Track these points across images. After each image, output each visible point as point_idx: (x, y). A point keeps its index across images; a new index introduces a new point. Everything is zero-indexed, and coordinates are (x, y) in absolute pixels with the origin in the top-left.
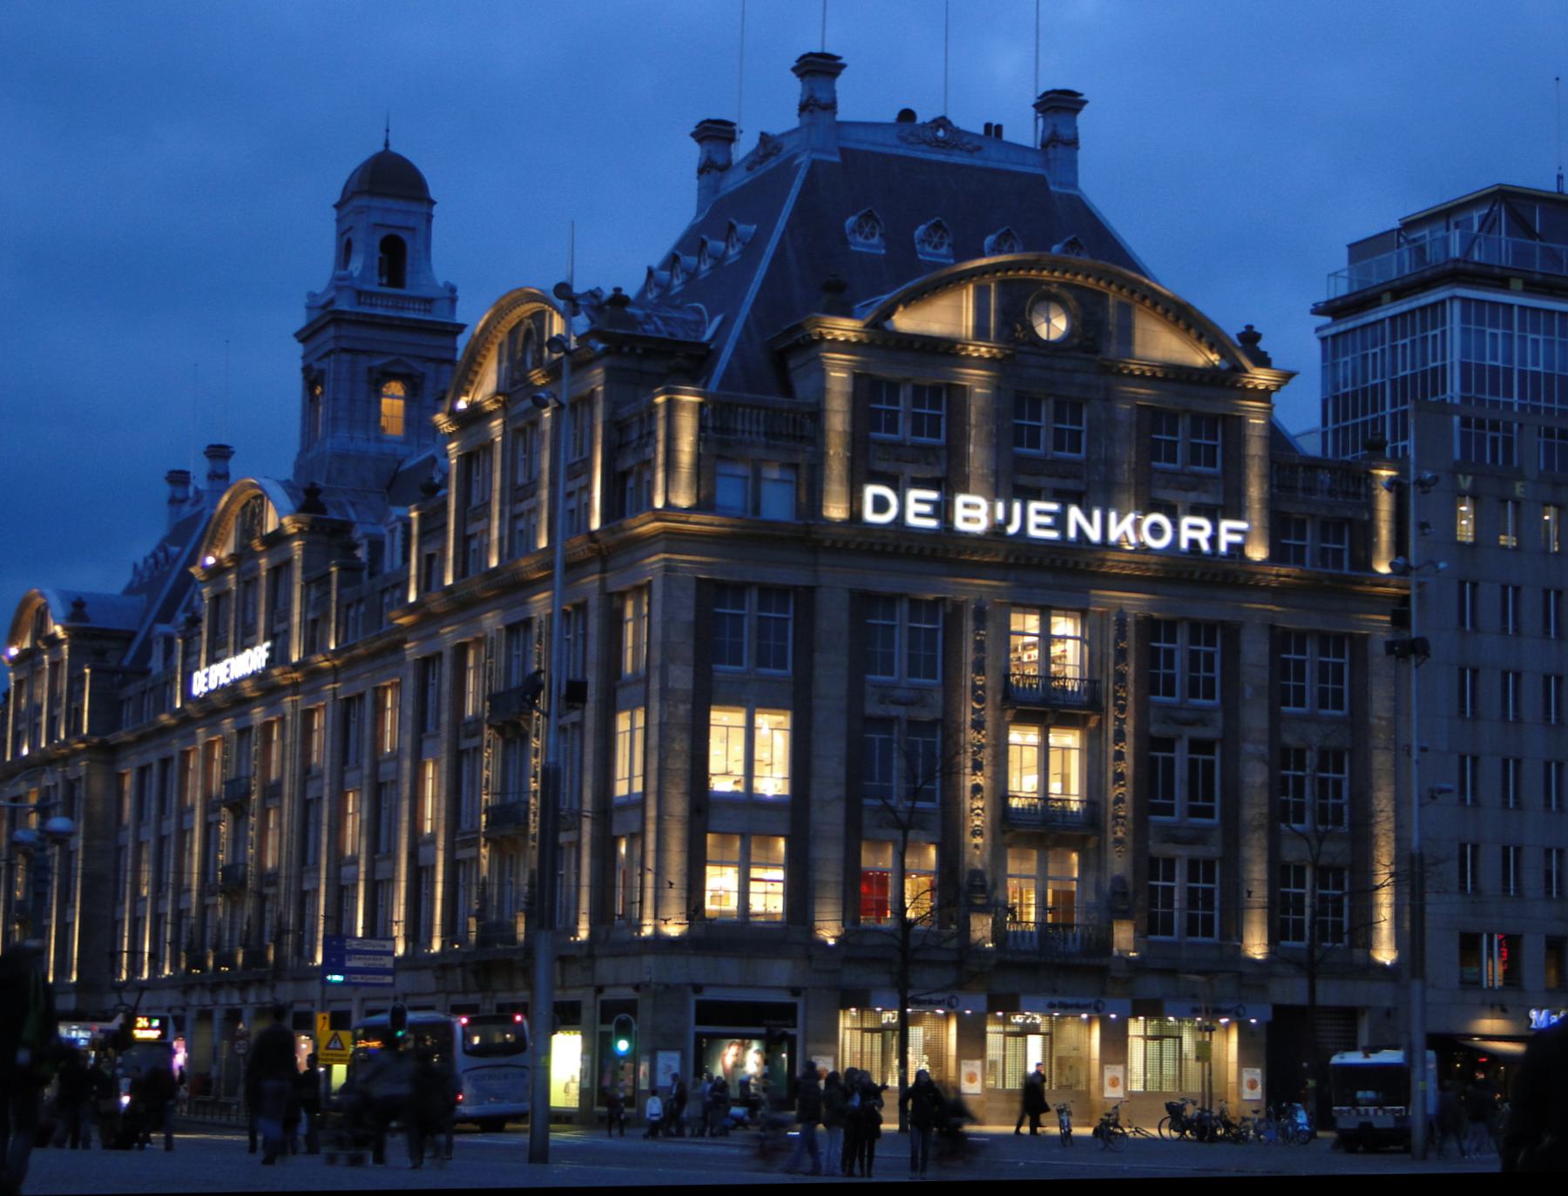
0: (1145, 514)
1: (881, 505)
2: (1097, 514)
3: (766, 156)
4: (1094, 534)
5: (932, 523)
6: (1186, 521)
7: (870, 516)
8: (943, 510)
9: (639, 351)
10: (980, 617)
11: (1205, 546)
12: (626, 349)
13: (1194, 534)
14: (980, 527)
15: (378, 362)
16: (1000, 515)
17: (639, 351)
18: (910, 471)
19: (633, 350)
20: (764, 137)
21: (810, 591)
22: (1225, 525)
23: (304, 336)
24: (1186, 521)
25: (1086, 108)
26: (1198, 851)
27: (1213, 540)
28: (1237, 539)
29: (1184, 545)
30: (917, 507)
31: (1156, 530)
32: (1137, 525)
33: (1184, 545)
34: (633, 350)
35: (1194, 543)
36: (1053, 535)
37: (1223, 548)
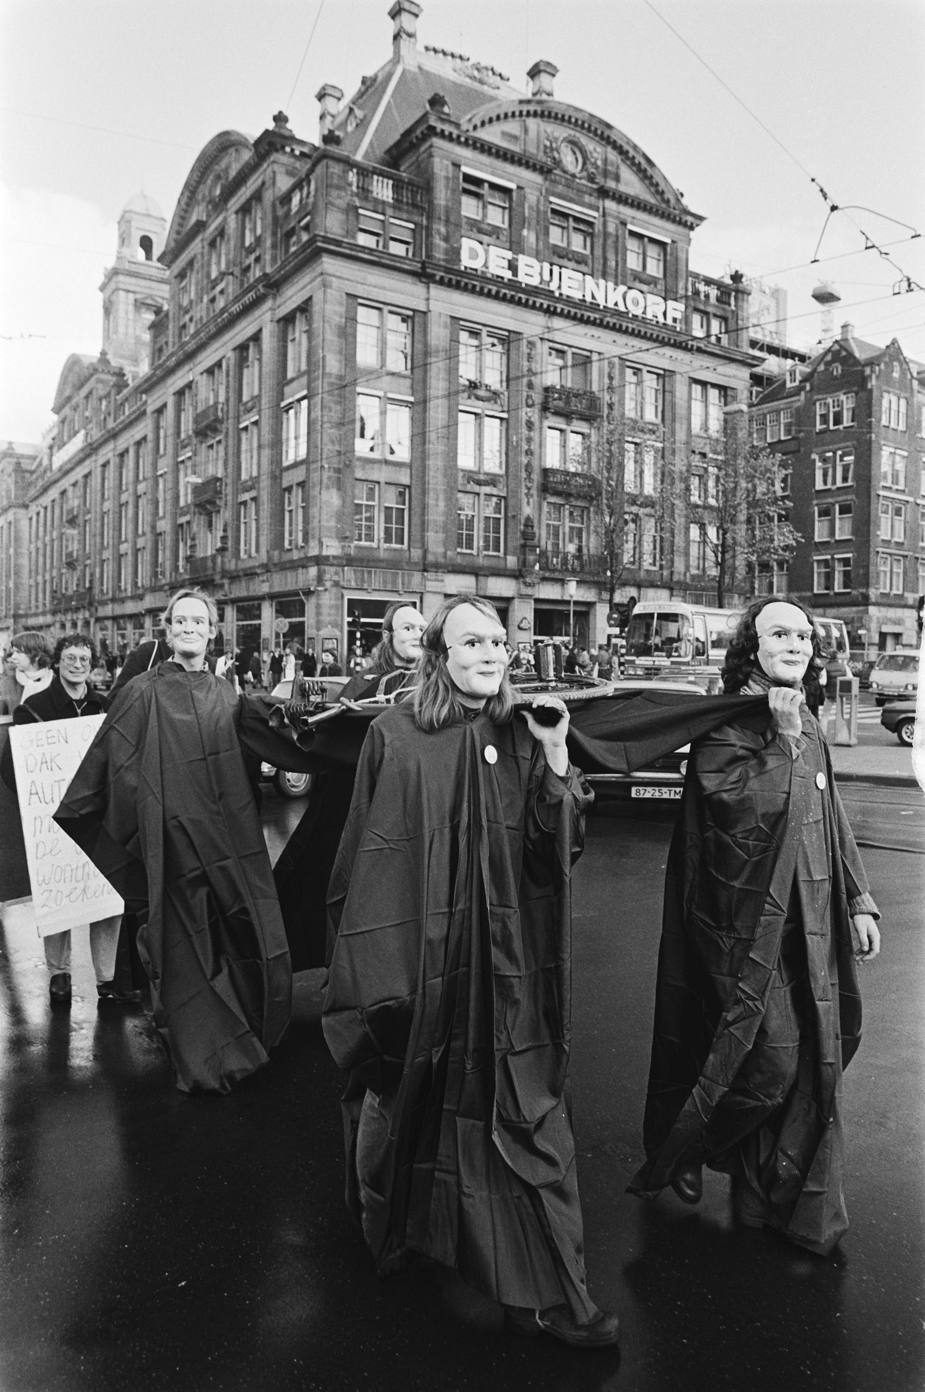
1: (474, 255)
3: (367, 90)
4: (601, 301)
5: (508, 275)
8: (513, 266)
9: (297, 153)
10: (531, 344)
12: (288, 149)
14: (535, 281)
15: (138, 296)
16: (546, 277)
17: (297, 153)
18: (486, 239)
19: (292, 150)
20: (364, 81)
21: (425, 313)
22: (671, 303)
23: (102, 288)
25: (558, 75)
27: (665, 314)
28: (679, 316)
34: (292, 150)
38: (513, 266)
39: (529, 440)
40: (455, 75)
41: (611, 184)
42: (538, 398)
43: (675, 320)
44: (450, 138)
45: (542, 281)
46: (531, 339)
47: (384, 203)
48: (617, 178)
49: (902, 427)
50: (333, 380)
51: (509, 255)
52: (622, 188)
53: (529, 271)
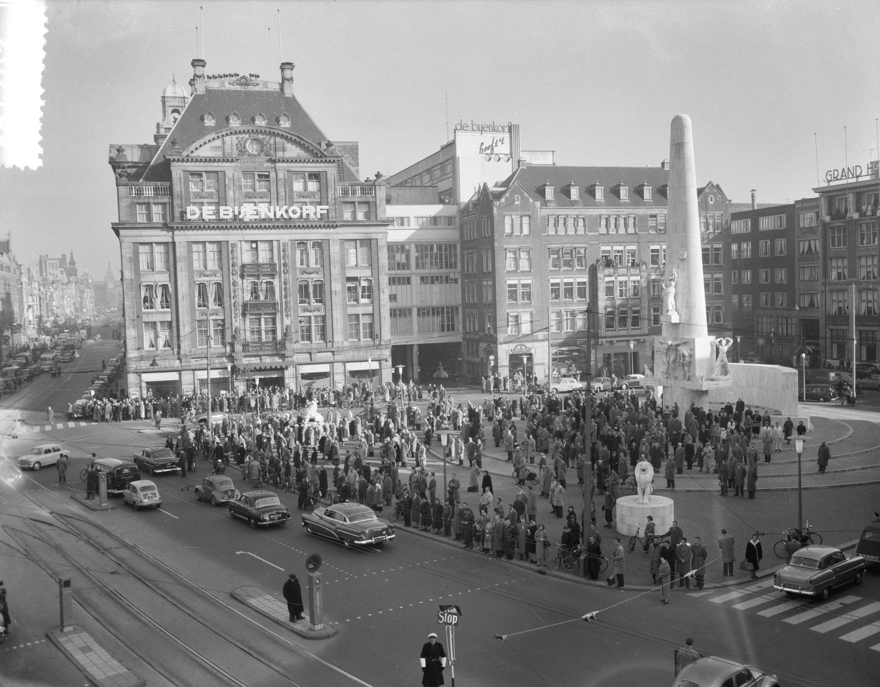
0: (290, 207)
2: (272, 208)
4: (271, 216)
5: (214, 217)
6: (304, 207)
7: (189, 217)
10: (234, 245)
11: (312, 216)
13: (308, 212)
16: (237, 213)
18: (205, 201)
22: (319, 207)
24: (304, 207)
26: (316, 313)
27: (315, 214)
28: (325, 212)
29: (304, 216)
30: (208, 212)
31: (294, 212)
32: (287, 211)
33: (304, 216)
35: (308, 215)
36: (257, 217)
37: (319, 216)
38: (217, 212)
39: (234, 291)
40: (231, 86)
41: (280, 154)
42: (238, 269)
43: (321, 214)
44: (179, 160)
45: (235, 216)
46: (233, 242)
47: (149, 197)
48: (284, 150)
49: (526, 231)
50: (128, 281)
51: (213, 208)
52: (287, 155)
53: (226, 212)
